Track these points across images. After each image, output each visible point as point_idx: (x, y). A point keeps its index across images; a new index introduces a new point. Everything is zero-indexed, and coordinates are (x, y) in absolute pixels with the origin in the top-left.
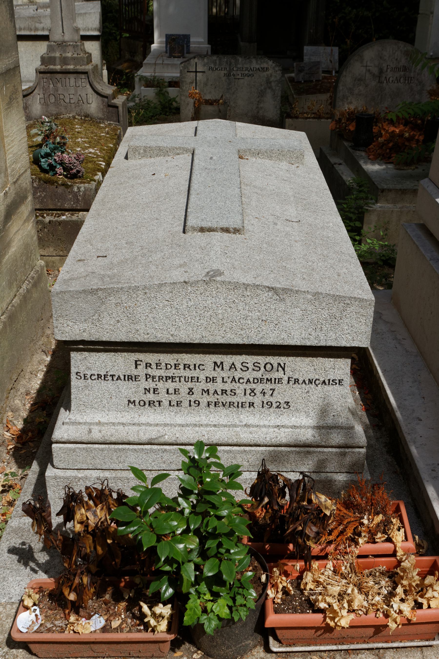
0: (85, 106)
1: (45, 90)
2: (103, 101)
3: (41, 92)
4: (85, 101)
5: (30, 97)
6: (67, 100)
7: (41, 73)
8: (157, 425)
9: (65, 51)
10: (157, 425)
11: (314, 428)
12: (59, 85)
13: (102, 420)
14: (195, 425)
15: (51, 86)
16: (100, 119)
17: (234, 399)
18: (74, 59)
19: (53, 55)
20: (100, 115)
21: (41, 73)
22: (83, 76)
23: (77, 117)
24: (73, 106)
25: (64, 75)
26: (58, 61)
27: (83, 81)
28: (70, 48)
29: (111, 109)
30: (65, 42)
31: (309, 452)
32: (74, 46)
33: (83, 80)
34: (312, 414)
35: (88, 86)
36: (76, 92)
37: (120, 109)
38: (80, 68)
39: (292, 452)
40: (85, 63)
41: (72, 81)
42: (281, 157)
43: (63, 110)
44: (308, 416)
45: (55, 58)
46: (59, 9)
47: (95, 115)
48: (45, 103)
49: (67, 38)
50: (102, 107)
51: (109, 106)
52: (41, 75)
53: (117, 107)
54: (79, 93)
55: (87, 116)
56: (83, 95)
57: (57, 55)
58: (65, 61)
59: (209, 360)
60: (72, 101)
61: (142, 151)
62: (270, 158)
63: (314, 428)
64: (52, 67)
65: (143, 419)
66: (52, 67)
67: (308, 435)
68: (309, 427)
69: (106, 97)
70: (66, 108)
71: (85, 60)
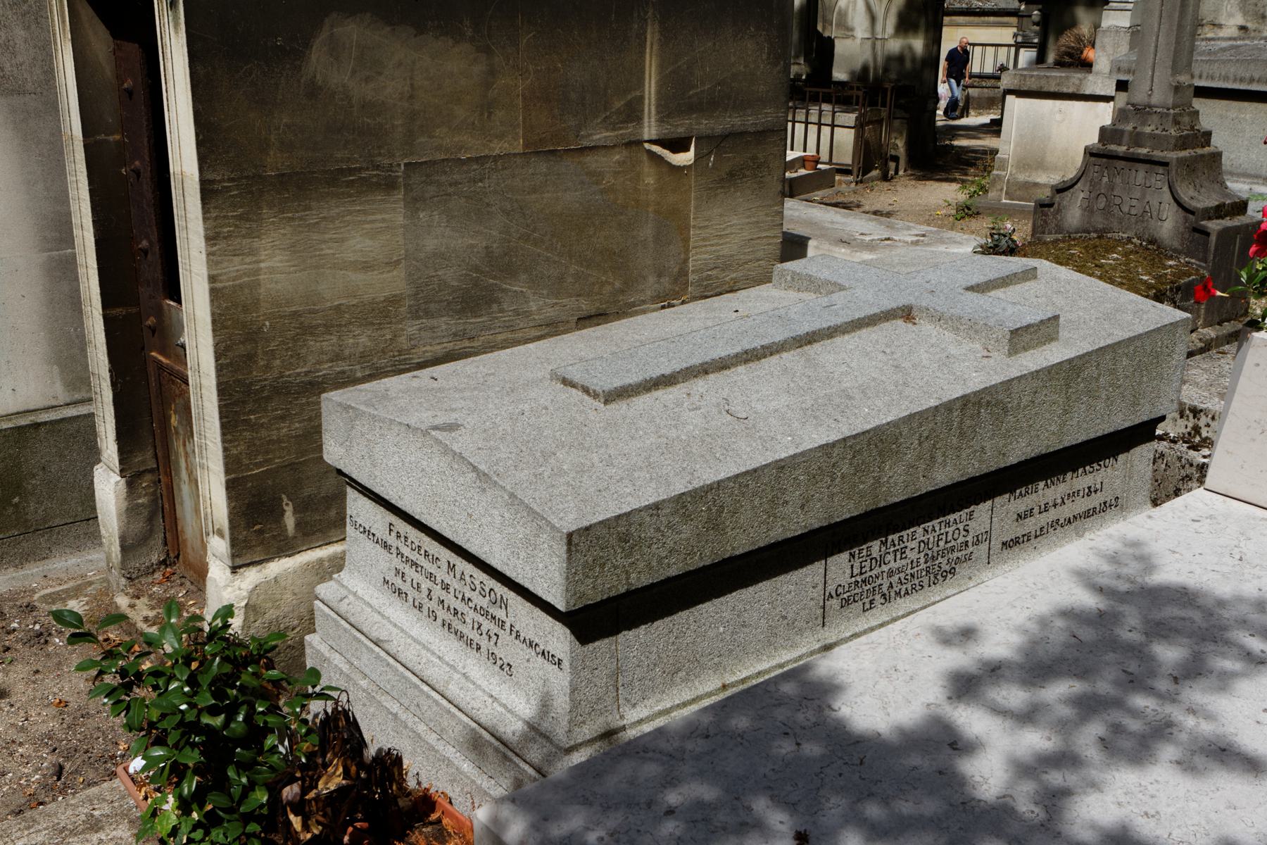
0: (1152, 222)
1: (1094, 185)
2: (1186, 220)
3: (1087, 189)
4: (1155, 214)
5: (1068, 193)
6: (1125, 209)
7: (1092, 155)
8: (395, 625)
9: (1144, 124)
10: (395, 625)
11: (528, 723)
12: (1118, 180)
13: (360, 593)
14: (424, 647)
15: (1105, 180)
16: (1175, 250)
17: (460, 627)
18: (1152, 136)
19: (1121, 127)
20: (1176, 244)
21: (1092, 155)
22: (1161, 170)
23: (1135, 240)
24: (1133, 219)
25: (1129, 164)
26: (1126, 138)
27: (1158, 179)
28: (1155, 117)
29: (1197, 235)
30: (1150, 107)
31: (505, 757)
32: (1162, 115)
33: (1159, 177)
34: (533, 702)
35: (1166, 189)
36: (1144, 196)
37: (1213, 238)
38: (1158, 154)
39: (491, 744)
40: (1171, 146)
41: (1141, 174)
42: (972, 333)
43: (1115, 225)
44: (528, 701)
45: (1122, 132)
46: (1152, 48)
47: (1167, 242)
48: (1089, 210)
49: (1155, 100)
50: (1181, 229)
51: (1195, 230)
52: (1093, 159)
53: (1208, 234)
54: (1148, 198)
55: (1152, 241)
56: (1155, 203)
57: (1129, 128)
58: (1137, 139)
59: (446, 554)
60: (1133, 212)
61: (789, 278)
62: (956, 330)
63: (528, 723)
64: (1113, 147)
65: (389, 612)
66: (1113, 147)
67: (512, 728)
68: (520, 719)
69: (1193, 213)
70: (1121, 221)
71: (1173, 141)
